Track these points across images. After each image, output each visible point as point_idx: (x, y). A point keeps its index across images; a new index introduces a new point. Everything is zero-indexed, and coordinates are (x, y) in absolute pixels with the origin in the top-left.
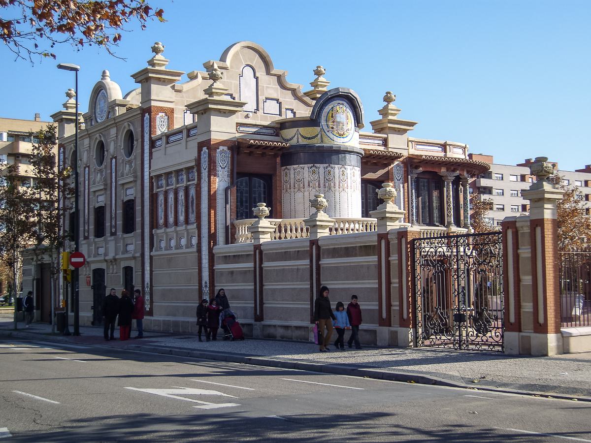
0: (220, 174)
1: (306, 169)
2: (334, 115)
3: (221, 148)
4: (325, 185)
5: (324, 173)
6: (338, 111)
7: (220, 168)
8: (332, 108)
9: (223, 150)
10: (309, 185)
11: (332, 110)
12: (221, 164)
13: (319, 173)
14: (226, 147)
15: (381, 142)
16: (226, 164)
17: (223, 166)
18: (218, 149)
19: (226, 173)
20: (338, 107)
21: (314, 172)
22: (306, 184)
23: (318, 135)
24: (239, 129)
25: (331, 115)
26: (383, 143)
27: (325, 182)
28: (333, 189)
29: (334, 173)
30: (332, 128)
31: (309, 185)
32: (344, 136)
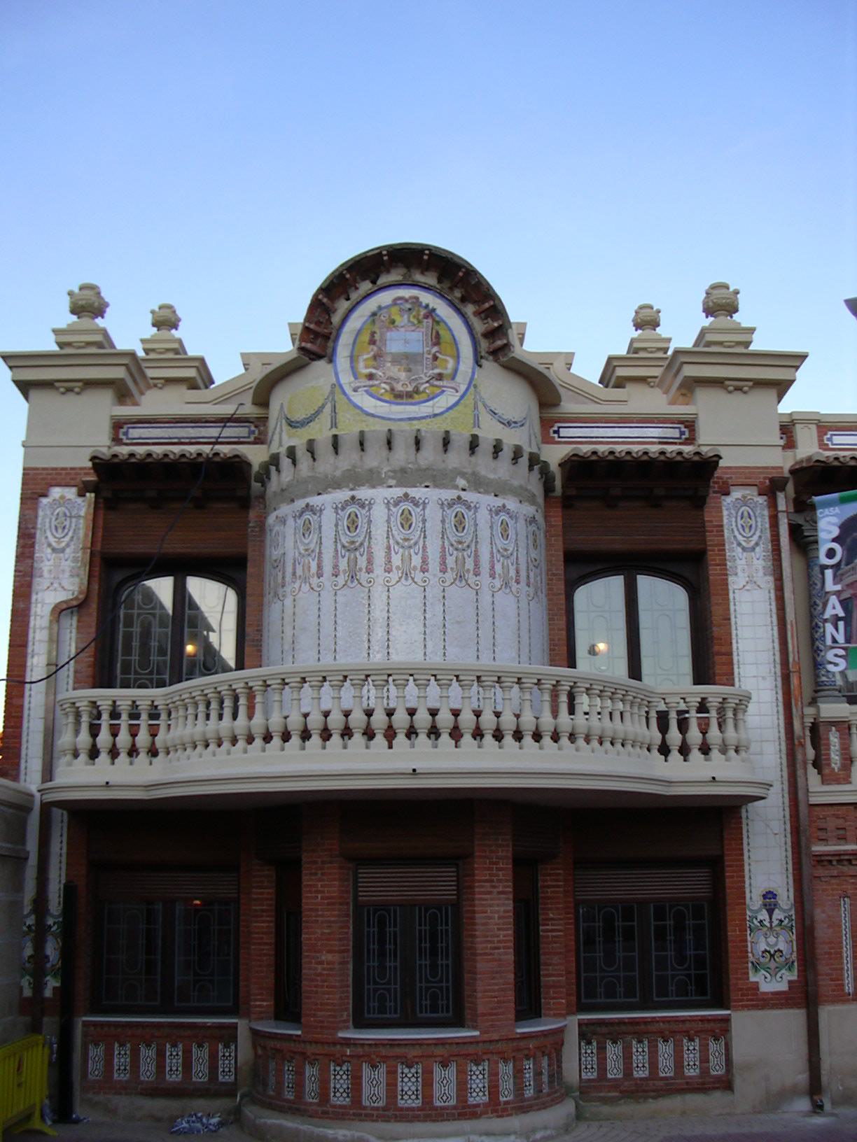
0: (46, 569)
1: (290, 522)
2: (377, 337)
3: (56, 492)
4: (336, 566)
5: (336, 525)
6: (393, 322)
7: (49, 550)
8: (374, 314)
9: (62, 497)
10: (294, 574)
11: (374, 322)
12: (52, 540)
13: (320, 527)
14: (74, 490)
15: (676, 433)
16: (67, 539)
17: (58, 543)
18: (45, 496)
19: (67, 565)
20: (394, 310)
21: (307, 528)
22: (289, 570)
23: (323, 406)
24: (126, 434)
25: (366, 337)
26: (682, 433)
27: (336, 557)
28: (363, 576)
29: (370, 522)
30: (371, 377)
31: (294, 574)
32: (417, 398)
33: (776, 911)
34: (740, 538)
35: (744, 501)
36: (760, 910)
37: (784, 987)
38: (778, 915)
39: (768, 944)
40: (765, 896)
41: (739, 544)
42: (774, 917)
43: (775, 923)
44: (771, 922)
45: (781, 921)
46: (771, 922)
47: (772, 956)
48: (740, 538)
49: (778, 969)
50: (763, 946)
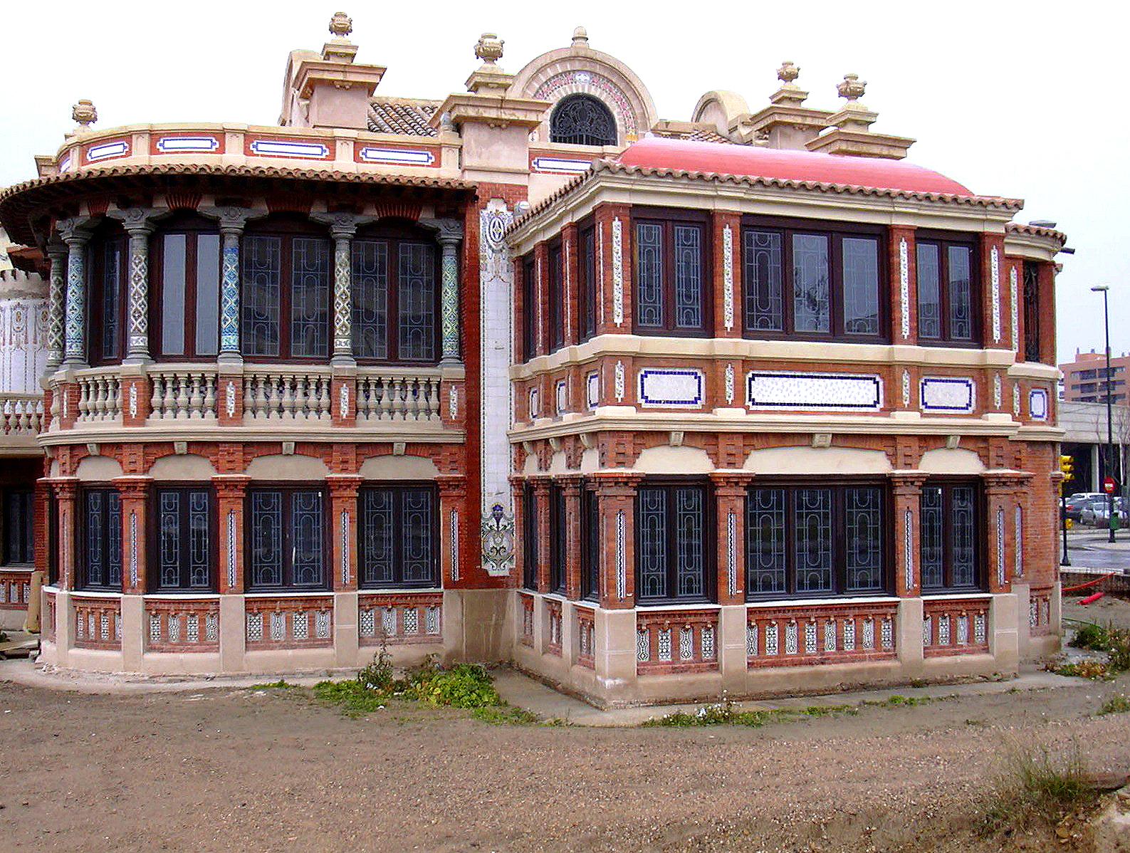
33: (502, 519)
34: (490, 241)
35: (497, 213)
36: (491, 518)
37: (506, 573)
38: (502, 522)
39: (495, 542)
40: (494, 509)
41: (490, 247)
42: (500, 523)
43: (501, 528)
44: (498, 527)
45: (505, 526)
46: (498, 527)
47: (498, 551)
48: (490, 241)
49: (502, 560)
50: (492, 544)
